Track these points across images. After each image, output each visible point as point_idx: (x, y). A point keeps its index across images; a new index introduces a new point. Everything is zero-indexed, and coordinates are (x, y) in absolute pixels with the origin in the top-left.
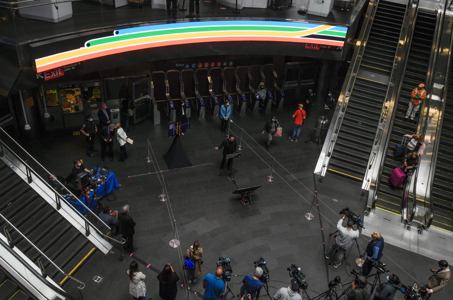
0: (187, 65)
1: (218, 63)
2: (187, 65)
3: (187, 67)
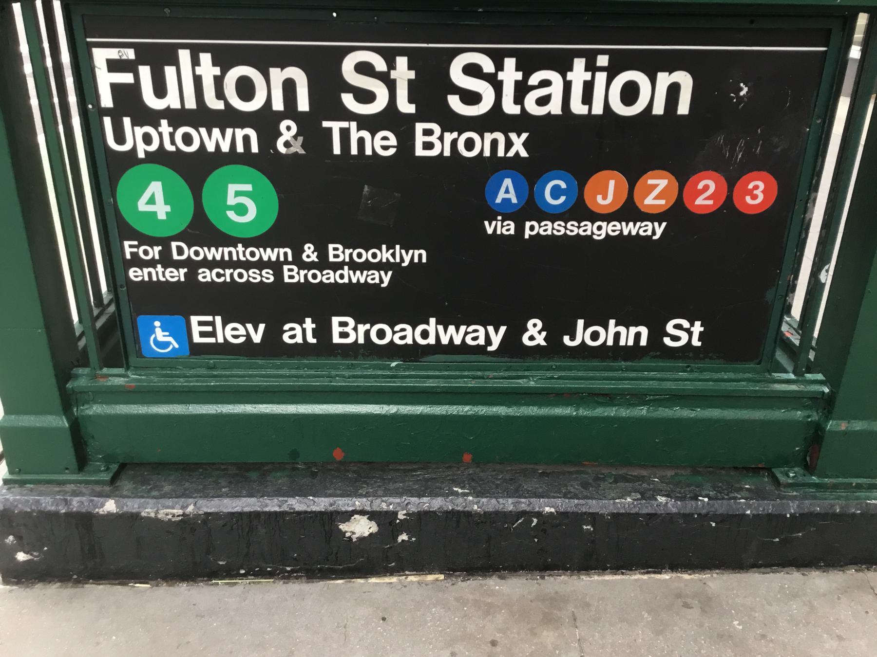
0: (508, 182)
1: (751, 186)
2: (508, 182)
3: (506, 201)
